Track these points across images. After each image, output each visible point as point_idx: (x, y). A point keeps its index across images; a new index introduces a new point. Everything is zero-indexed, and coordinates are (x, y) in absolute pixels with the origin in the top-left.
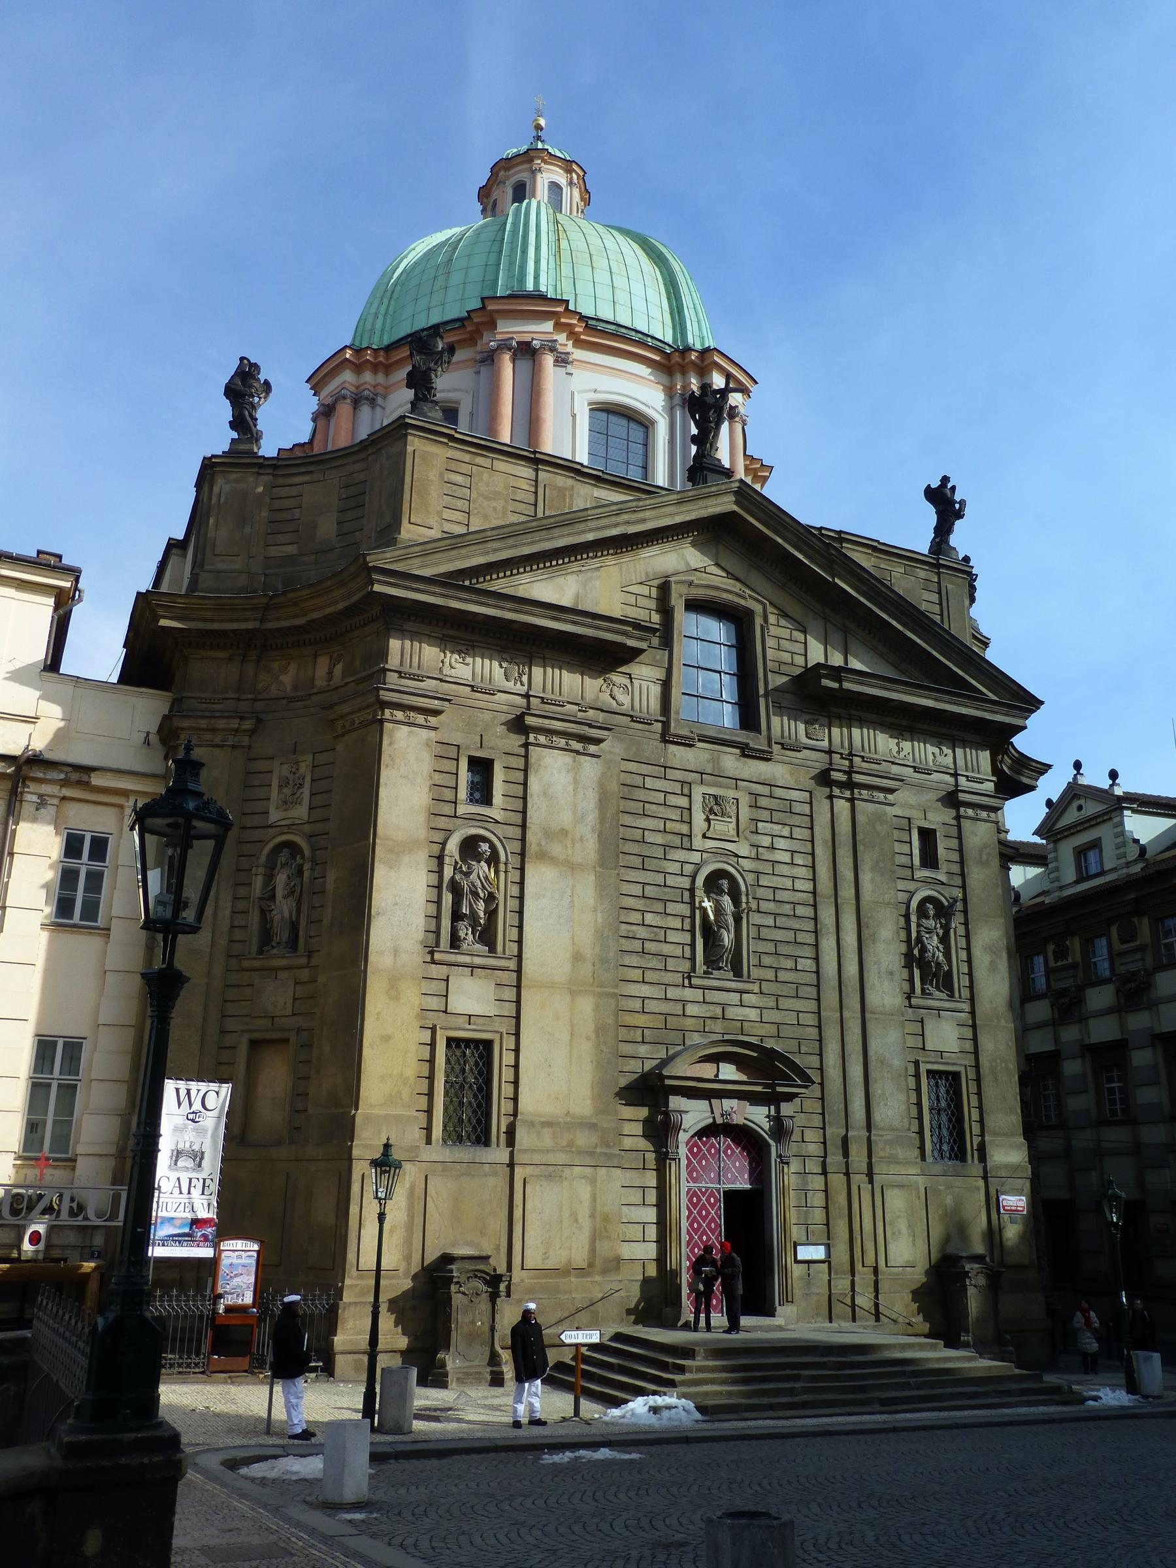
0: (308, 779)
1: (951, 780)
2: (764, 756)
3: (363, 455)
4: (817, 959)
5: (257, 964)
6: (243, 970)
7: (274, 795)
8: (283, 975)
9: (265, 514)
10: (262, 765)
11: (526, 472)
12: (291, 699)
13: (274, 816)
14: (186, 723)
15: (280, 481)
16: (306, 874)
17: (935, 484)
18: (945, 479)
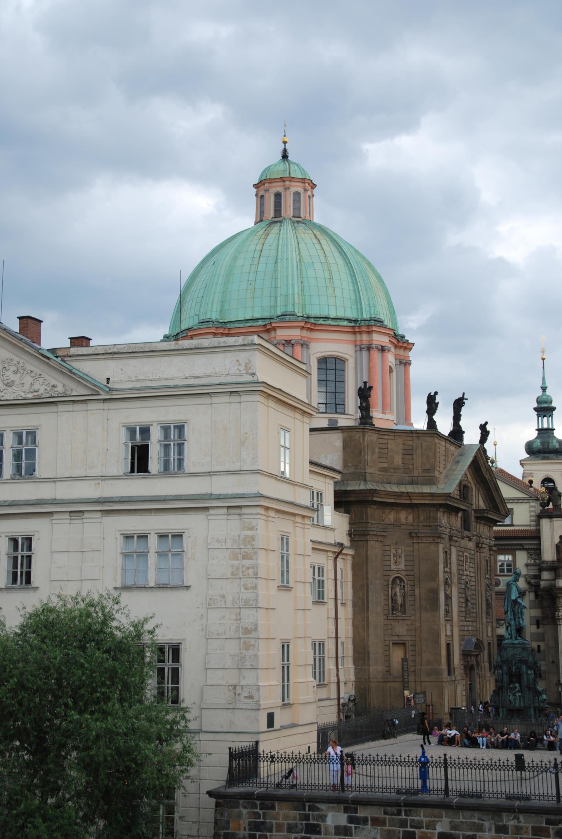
0: (403, 555)
1: (488, 541)
2: (470, 540)
3: (411, 435)
4: (476, 608)
5: (393, 618)
6: (388, 619)
7: (392, 560)
8: (401, 622)
9: (377, 450)
10: (387, 548)
11: (443, 443)
12: (394, 525)
13: (393, 567)
14: (371, 533)
15: (380, 437)
16: (406, 589)
17: (483, 423)
18: (486, 423)
